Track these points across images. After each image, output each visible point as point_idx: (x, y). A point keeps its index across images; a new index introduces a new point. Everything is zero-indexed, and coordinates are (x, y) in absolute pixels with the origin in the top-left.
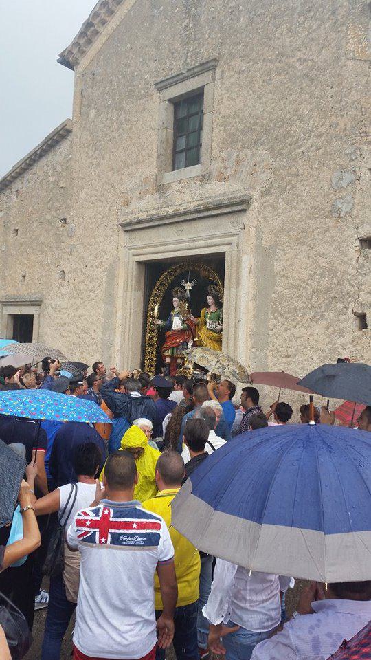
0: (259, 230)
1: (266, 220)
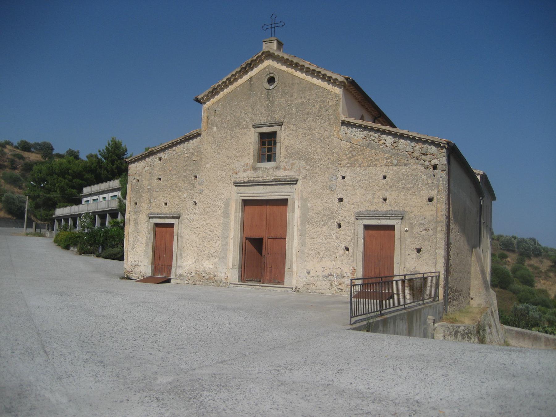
0: (302, 191)
1: (305, 188)
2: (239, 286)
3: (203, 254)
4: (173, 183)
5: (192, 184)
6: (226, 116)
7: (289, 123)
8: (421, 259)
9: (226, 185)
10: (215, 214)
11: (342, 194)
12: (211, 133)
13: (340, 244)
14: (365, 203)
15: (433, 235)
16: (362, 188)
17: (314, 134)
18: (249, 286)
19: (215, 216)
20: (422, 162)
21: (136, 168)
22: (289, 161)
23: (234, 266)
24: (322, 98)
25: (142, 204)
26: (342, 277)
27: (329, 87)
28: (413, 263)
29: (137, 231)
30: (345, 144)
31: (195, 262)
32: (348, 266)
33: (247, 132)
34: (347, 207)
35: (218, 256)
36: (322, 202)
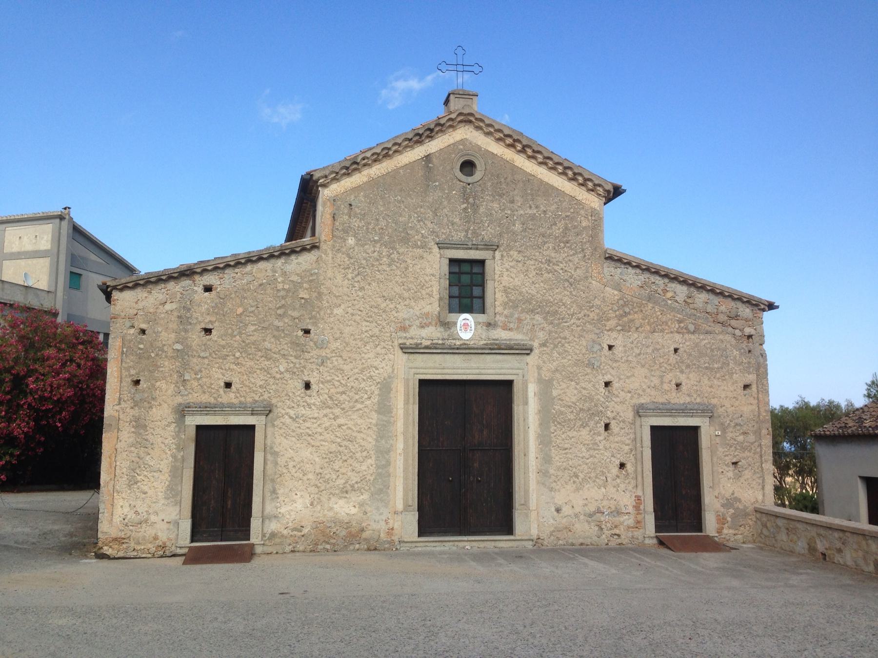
0: (539, 368)
1: (544, 362)
2: (421, 544)
3: (331, 488)
4: (247, 341)
5: (298, 345)
6: (377, 220)
7: (509, 248)
8: (742, 480)
9: (383, 351)
10: (359, 406)
11: (612, 376)
12: (342, 247)
13: (613, 459)
14: (648, 390)
15: (755, 442)
16: (643, 366)
17: (556, 271)
18: (444, 544)
19: (357, 410)
20: (730, 329)
21: (136, 303)
22: (512, 315)
23: (407, 507)
24: (569, 213)
25: (158, 384)
26: (619, 513)
27: (582, 194)
28: (729, 485)
29: (142, 443)
30: (611, 293)
31: (312, 504)
32: (628, 494)
33: (425, 255)
34: (620, 395)
35: (367, 488)
36: (578, 387)
